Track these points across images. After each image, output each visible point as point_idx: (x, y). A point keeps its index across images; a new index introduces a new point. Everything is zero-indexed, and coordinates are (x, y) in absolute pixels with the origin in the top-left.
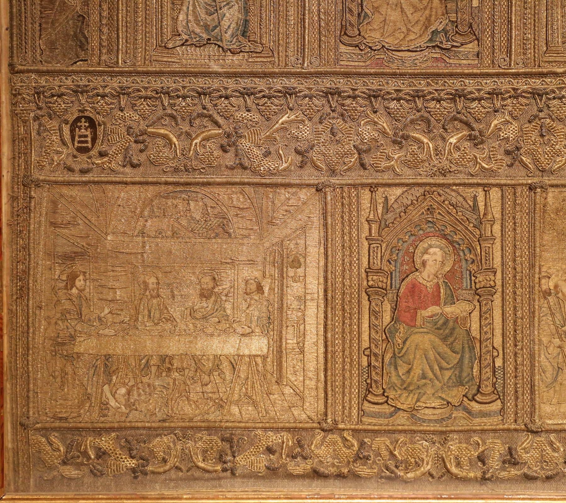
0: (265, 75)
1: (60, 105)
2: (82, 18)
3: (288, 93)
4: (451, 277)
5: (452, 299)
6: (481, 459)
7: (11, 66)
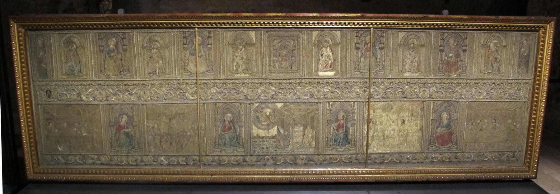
0: (85, 81)
1: (43, 88)
2: (46, 70)
3: (90, 85)
4: (127, 123)
5: (128, 128)
6: (136, 161)
7: (33, 80)
